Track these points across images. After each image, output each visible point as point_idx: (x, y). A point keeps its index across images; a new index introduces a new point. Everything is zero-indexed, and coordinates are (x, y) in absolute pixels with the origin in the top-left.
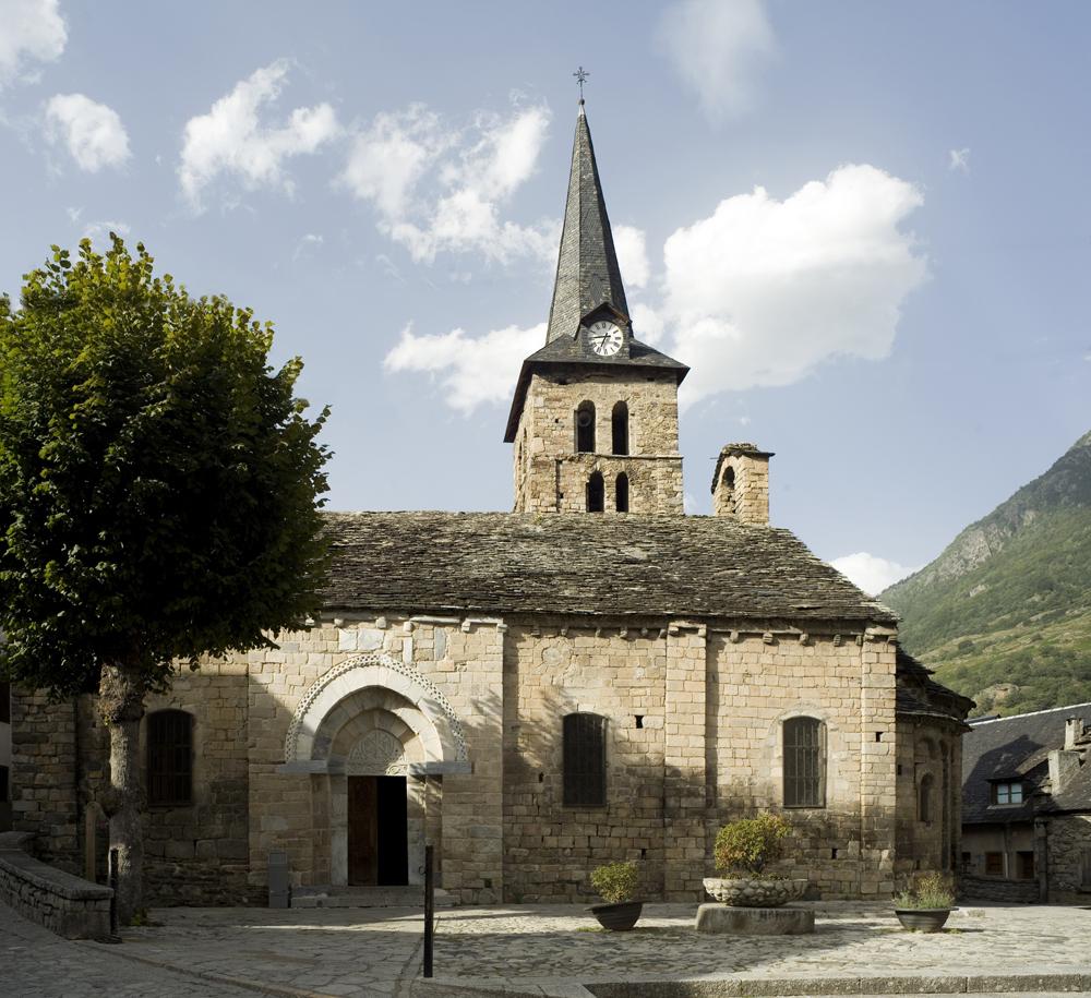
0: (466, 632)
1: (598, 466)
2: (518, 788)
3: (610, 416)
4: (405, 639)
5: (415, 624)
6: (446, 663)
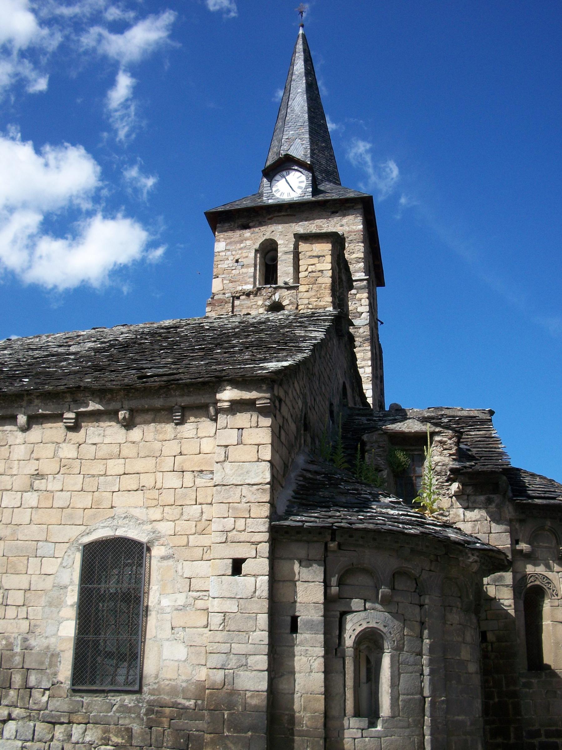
1: (276, 297)
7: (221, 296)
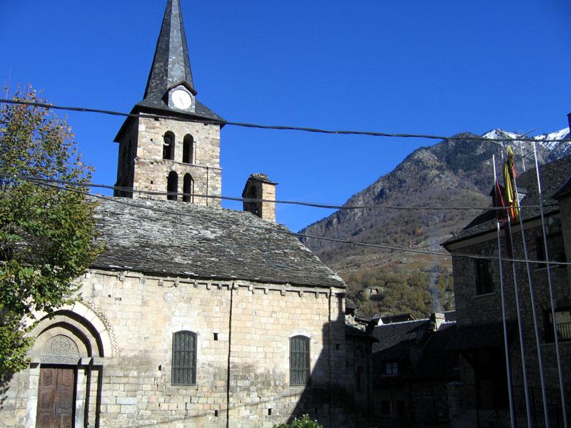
1: (174, 168)
2: (147, 374)
3: (182, 141)
7: (143, 160)
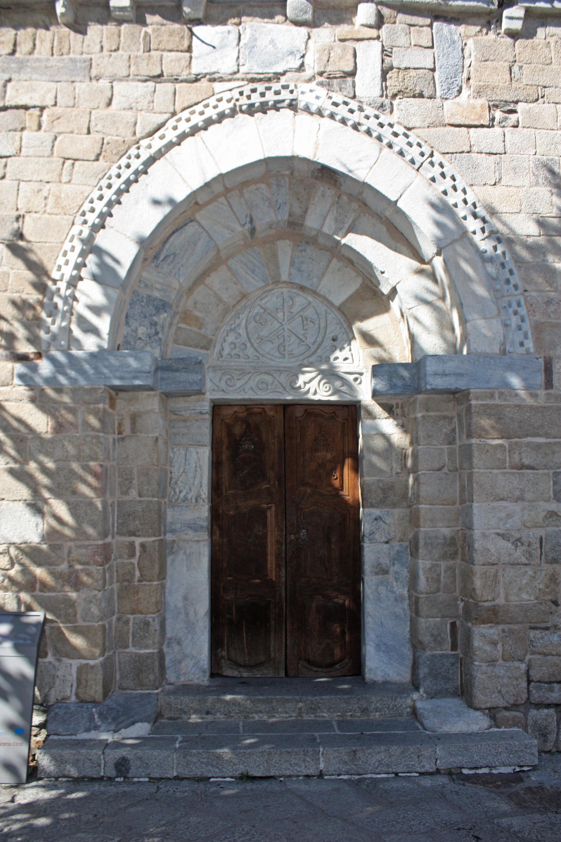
0: (513, 35)
4: (360, 46)
5: (386, 11)
6: (466, 105)
